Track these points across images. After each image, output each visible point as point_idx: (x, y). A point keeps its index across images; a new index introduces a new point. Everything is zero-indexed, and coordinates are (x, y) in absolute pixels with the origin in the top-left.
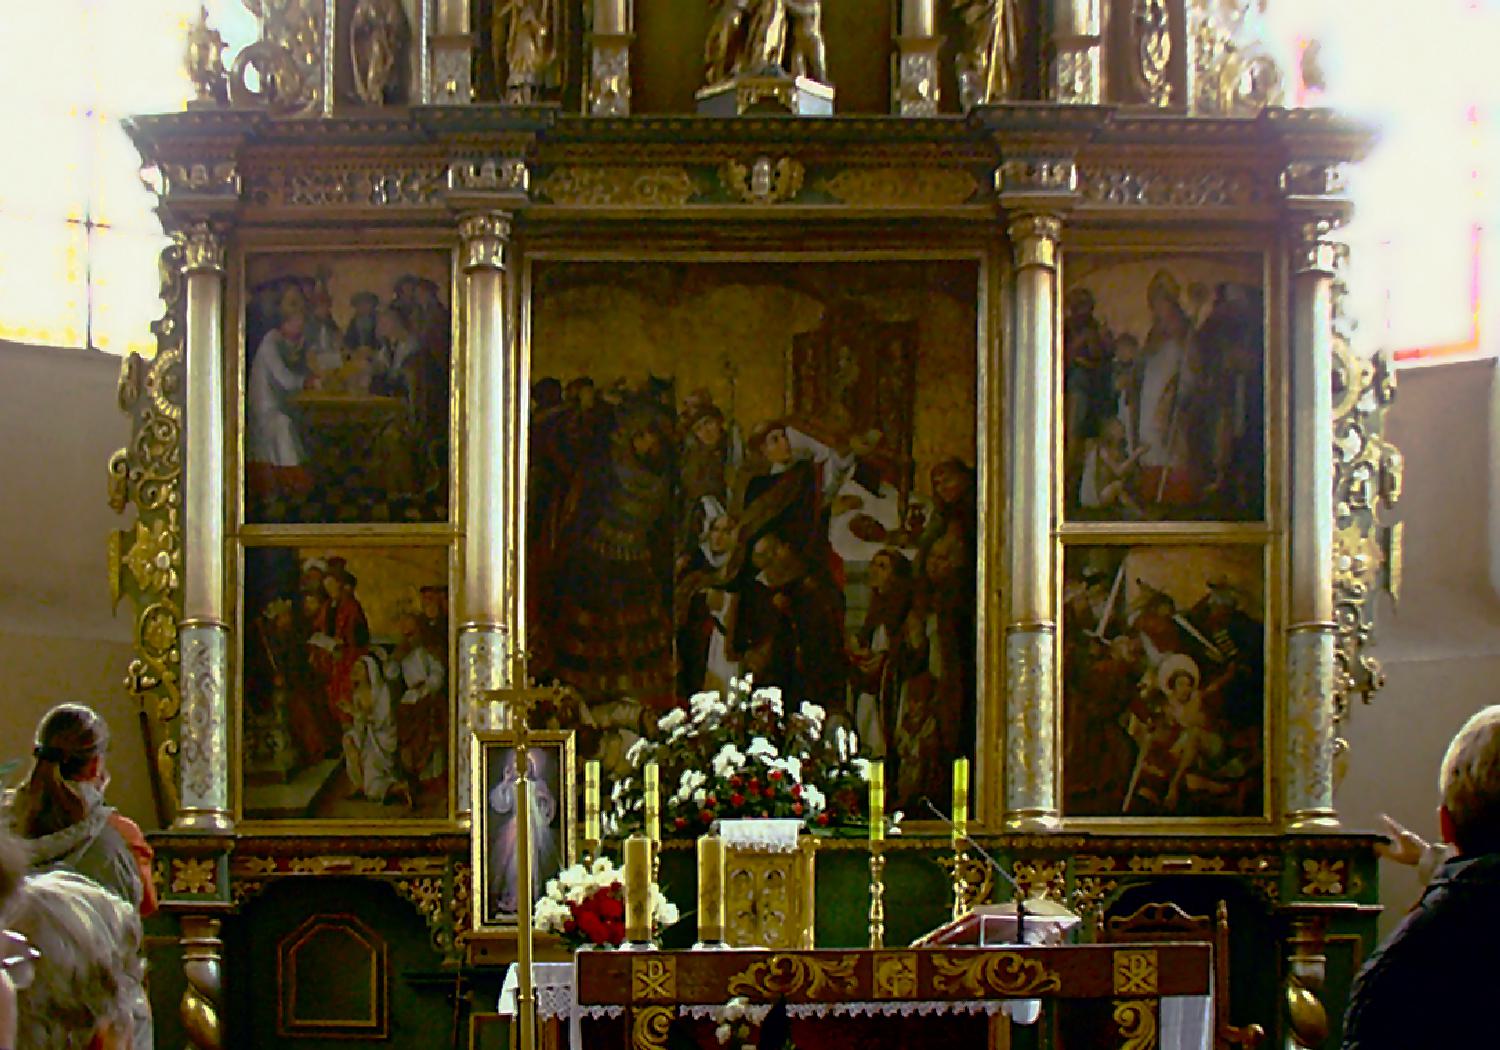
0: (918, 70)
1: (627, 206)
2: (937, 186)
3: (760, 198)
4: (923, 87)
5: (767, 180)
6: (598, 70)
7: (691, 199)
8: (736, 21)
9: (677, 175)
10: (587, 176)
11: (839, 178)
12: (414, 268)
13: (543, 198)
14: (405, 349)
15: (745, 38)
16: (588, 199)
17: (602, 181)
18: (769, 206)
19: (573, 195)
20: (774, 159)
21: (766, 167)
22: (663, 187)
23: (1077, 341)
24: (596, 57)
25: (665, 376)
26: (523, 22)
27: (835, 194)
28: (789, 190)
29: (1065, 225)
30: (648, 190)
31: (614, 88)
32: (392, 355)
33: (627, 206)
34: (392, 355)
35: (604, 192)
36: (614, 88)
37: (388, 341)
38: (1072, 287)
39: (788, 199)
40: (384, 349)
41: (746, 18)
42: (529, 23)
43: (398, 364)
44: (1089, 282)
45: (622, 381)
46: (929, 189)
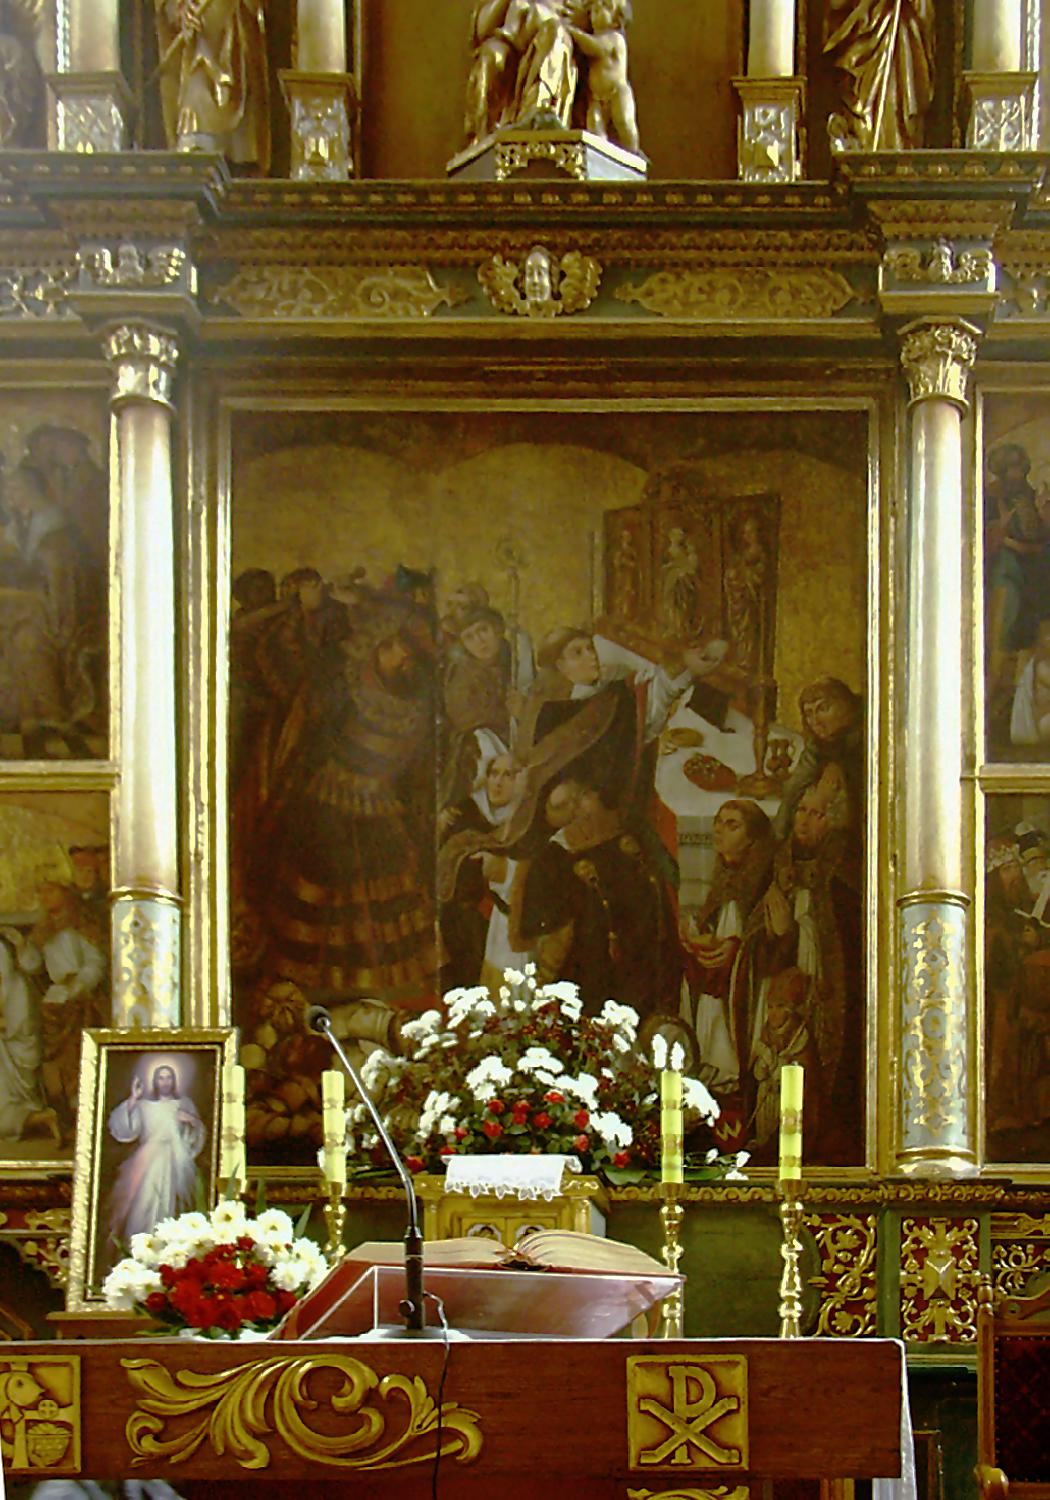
0: (767, 128)
1: (346, 319)
2: (795, 293)
3: (537, 307)
4: (773, 152)
5: (546, 282)
6: (300, 128)
7: (440, 308)
8: (499, 58)
9: (420, 278)
10: (287, 277)
11: (652, 282)
12: (55, 415)
13: (225, 309)
14: (42, 523)
15: (511, 84)
16: (290, 309)
17: (309, 285)
18: (552, 319)
19: (268, 306)
20: (555, 250)
21: (545, 264)
22: (396, 294)
23: (1005, 518)
24: (298, 111)
25: (422, 566)
26: (194, 64)
27: (645, 303)
28: (581, 296)
29: (984, 350)
30: (376, 298)
31: (324, 152)
32: (23, 534)
33: (346, 319)
34: (23, 534)
35: (313, 301)
36: (324, 152)
37: (17, 512)
38: (994, 446)
39: (579, 311)
40: (13, 524)
41: (514, 55)
42: (201, 64)
43: (33, 545)
44: (1022, 437)
45: (360, 573)
46: (783, 297)
